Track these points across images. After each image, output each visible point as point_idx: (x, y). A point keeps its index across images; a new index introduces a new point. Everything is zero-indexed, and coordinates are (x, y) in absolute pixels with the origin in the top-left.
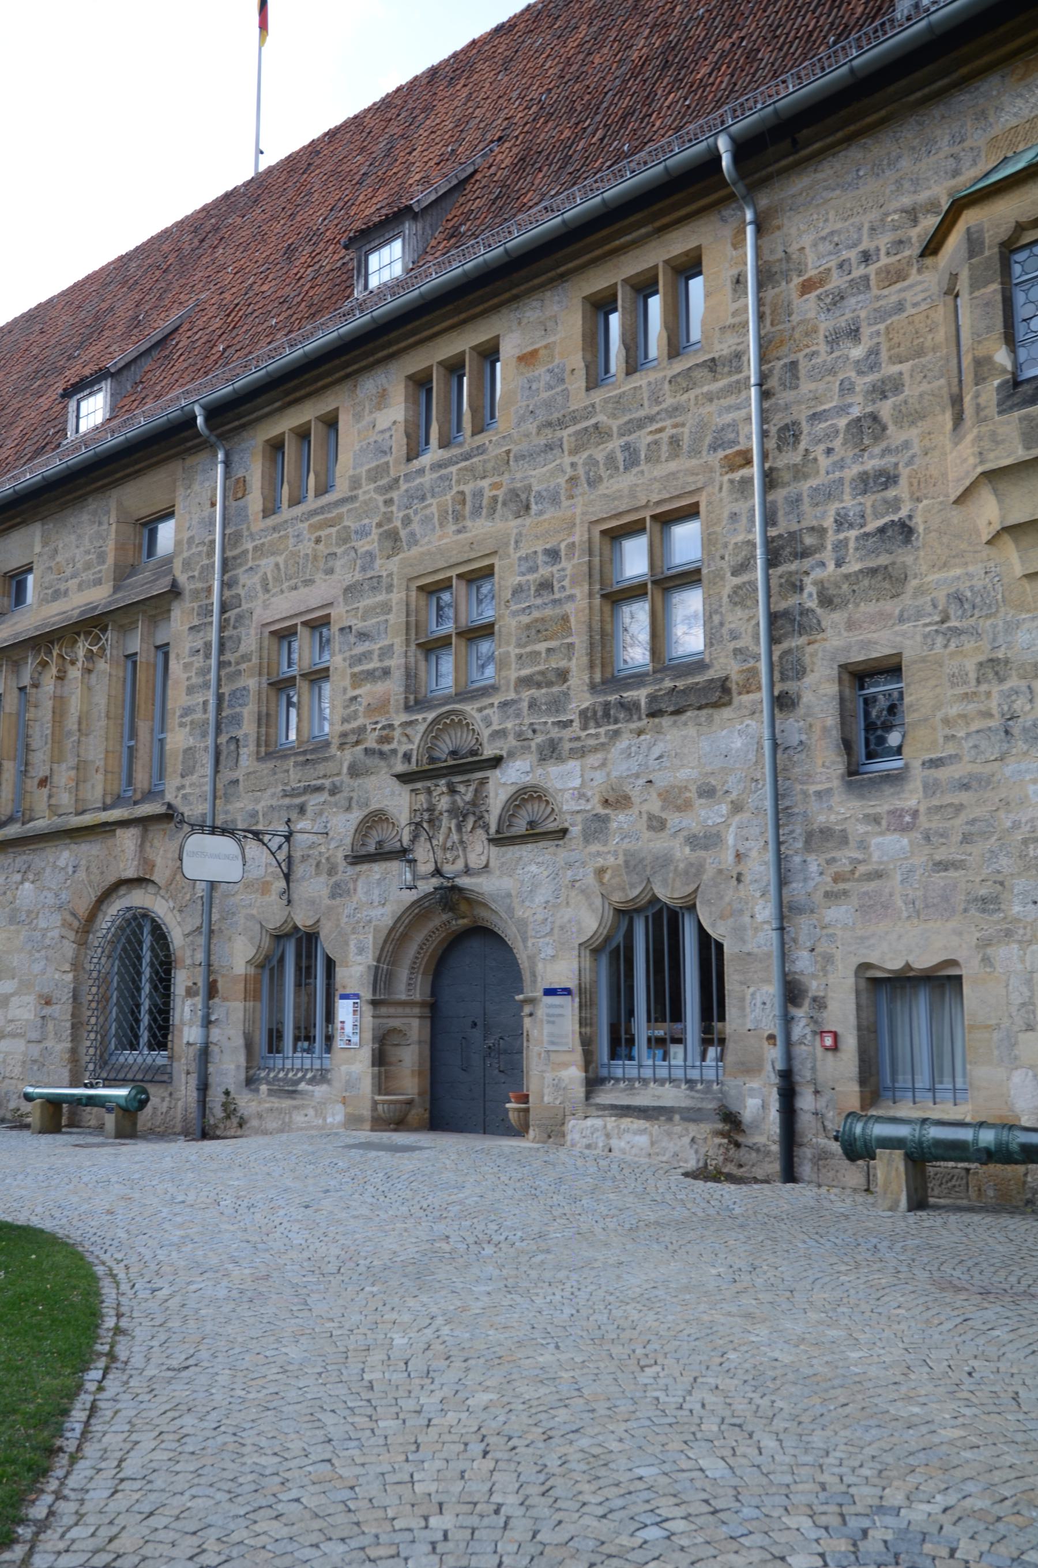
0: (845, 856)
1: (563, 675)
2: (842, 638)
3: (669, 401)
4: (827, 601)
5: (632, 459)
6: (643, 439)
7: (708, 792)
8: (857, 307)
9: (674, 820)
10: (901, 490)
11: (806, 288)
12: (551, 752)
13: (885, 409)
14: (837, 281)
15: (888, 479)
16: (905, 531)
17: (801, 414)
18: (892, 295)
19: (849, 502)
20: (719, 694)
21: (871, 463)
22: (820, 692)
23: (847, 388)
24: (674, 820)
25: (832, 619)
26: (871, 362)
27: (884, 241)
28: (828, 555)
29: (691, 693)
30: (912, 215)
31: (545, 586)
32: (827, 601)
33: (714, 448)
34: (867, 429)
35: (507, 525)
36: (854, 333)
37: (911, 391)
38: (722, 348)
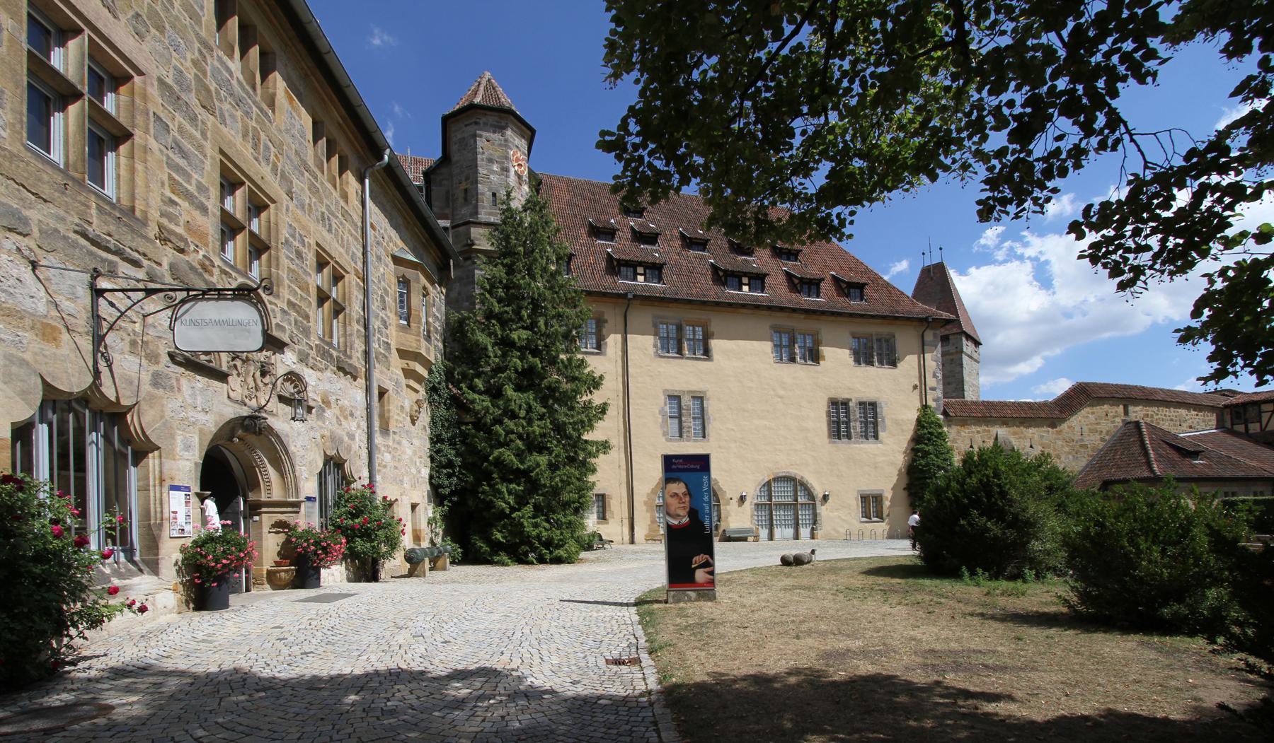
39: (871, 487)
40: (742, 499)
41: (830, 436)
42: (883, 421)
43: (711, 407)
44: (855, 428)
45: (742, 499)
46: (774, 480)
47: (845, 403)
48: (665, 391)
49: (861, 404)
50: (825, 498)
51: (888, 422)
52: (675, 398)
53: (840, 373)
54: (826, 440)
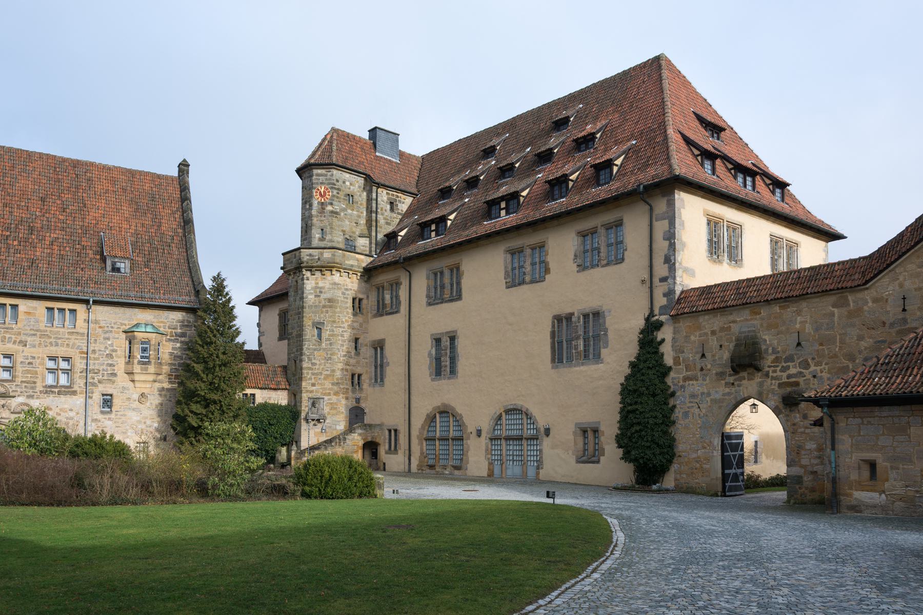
0: (99, 424)
1: (35, 383)
2: (101, 388)
3: (67, 336)
4: (99, 382)
5: (57, 345)
6: (60, 341)
7: (71, 410)
8: (111, 335)
9: (62, 414)
10: (115, 368)
11: (100, 327)
12: (31, 397)
13: (114, 354)
14: (106, 329)
15: (111, 365)
16: (115, 375)
17: (96, 349)
18: (117, 336)
19: (105, 367)
20: (74, 393)
21: (110, 362)
22: (97, 398)
23: (106, 348)
24: (62, 414)
25: (100, 385)
26: (112, 345)
27: (116, 326)
28: (100, 374)
29: (68, 391)
30: (122, 324)
31: (30, 363)
32: (99, 382)
33: (77, 348)
34: (110, 356)
35: (21, 348)
36: (108, 339)
37: (119, 352)
38: (81, 331)
39: (587, 416)
40: (479, 433)
41: (553, 360)
42: (606, 335)
43: (461, 343)
44: (576, 347)
45: (479, 433)
46: (508, 411)
47: (569, 317)
48: (432, 335)
49: (586, 316)
50: (547, 432)
51: (611, 335)
52: (438, 341)
53: (568, 280)
54: (549, 365)
